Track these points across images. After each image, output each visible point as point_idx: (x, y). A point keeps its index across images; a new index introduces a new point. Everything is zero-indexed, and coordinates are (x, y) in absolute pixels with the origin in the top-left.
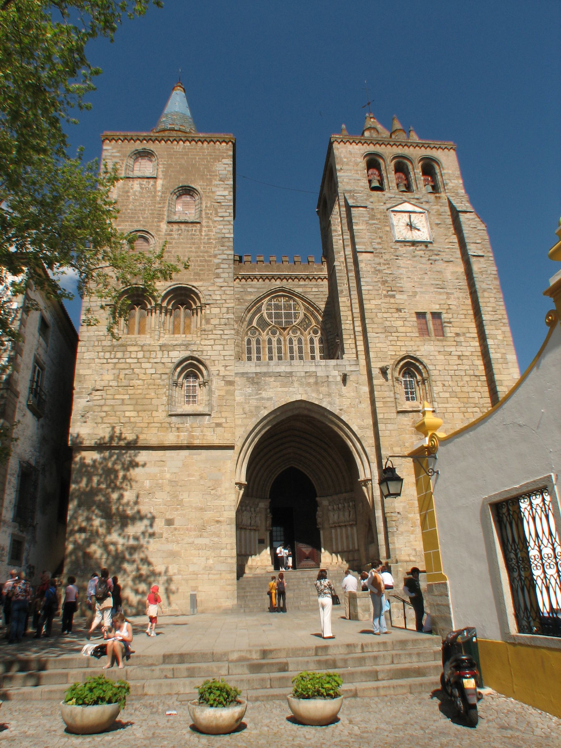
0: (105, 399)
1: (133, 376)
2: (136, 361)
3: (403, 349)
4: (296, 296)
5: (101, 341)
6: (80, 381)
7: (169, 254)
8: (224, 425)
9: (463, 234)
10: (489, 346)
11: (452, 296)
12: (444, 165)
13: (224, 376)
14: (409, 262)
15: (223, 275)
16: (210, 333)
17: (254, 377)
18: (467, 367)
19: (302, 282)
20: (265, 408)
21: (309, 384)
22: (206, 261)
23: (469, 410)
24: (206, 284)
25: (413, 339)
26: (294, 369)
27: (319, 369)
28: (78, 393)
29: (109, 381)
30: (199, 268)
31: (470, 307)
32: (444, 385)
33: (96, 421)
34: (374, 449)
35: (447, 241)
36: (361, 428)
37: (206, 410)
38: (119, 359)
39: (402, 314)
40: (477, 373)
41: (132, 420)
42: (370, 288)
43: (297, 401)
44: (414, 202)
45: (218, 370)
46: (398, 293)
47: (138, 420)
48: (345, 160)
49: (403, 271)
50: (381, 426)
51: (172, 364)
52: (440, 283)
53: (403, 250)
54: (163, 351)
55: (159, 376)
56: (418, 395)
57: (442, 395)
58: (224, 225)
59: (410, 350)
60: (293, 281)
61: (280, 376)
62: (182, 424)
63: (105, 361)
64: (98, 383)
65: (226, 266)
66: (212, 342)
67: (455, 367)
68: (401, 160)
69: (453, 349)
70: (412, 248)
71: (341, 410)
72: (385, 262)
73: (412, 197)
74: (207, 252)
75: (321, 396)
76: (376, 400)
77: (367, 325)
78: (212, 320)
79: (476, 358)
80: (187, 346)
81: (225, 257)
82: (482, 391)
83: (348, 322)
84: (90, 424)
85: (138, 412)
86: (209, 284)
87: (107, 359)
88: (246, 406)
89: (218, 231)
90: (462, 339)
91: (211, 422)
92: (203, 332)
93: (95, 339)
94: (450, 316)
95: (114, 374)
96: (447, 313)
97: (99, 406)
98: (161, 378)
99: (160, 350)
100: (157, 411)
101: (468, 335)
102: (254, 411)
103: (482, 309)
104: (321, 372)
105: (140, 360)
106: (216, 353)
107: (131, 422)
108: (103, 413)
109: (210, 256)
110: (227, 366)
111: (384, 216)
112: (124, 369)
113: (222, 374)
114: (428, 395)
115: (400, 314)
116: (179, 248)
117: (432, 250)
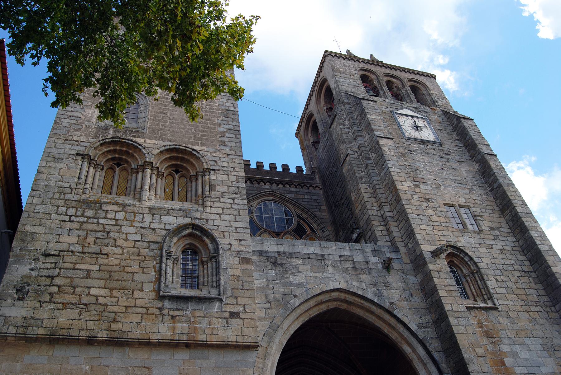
0: (60, 269)
1: (107, 241)
2: (113, 222)
3: (442, 238)
4: (287, 201)
5: (64, 194)
6: (23, 241)
7: (164, 115)
8: (243, 315)
9: (471, 136)
10: (534, 237)
11: (474, 192)
12: (430, 87)
13: (238, 252)
14: (424, 157)
15: (228, 144)
16: (217, 200)
17: (276, 258)
18: (513, 262)
19: (292, 189)
20: (295, 296)
21: (346, 271)
22: (208, 128)
23: (533, 309)
24: (207, 149)
25: (450, 229)
26: (326, 251)
27: (355, 254)
28: (16, 256)
29: (69, 244)
30: (201, 133)
31: (494, 204)
32: (497, 280)
33: (39, 299)
34: (442, 355)
35: (452, 144)
36: (419, 326)
37: (214, 293)
38: (89, 218)
39: (431, 204)
40: (525, 269)
41: (101, 300)
42: (398, 170)
43: (334, 290)
44: (414, 109)
45: (229, 244)
46: (421, 184)
47: (109, 301)
48: (342, 70)
49: (419, 164)
50: (453, 321)
51: (165, 232)
52: (459, 179)
53: (414, 146)
54: (153, 215)
55: (146, 245)
56: (469, 293)
57: (498, 290)
58: (227, 99)
59: (451, 240)
60: (284, 186)
61: (309, 258)
62: (178, 310)
63: (67, 218)
64: (50, 245)
65: (233, 136)
66: (220, 211)
67: (502, 261)
68: (390, 79)
69: (492, 242)
70: (422, 146)
71: (391, 303)
72: (401, 155)
73: (411, 106)
74: (209, 120)
75: (364, 285)
76: (438, 288)
77: (406, 206)
78: (218, 187)
79: (518, 253)
80: (185, 213)
81: (231, 127)
82: (537, 288)
83: (375, 208)
84: (29, 302)
85: (111, 290)
86: (213, 150)
87: (71, 216)
88: (270, 292)
89: (222, 103)
90: (497, 233)
91: (224, 310)
92: (208, 199)
93: (56, 190)
94: (479, 210)
95: (79, 236)
96: (474, 207)
97: (48, 277)
98: (148, 248)
99: (150, 213)
100: (142, 290)
101: (502, 230)
102: (281, 300)
103: (513, 201)
104: (359, 258)
105: (119, 222)
106: (227, 223)
107: (100, 304)
108: (52, 288)
109: (214, 124)
110: (241, 240)
111: (389, 116)
112: (96, 231)
113: (235, 247)
114: (483, 290)
115: (429, 203)
116: (176, 111)
117: (443, 150)
